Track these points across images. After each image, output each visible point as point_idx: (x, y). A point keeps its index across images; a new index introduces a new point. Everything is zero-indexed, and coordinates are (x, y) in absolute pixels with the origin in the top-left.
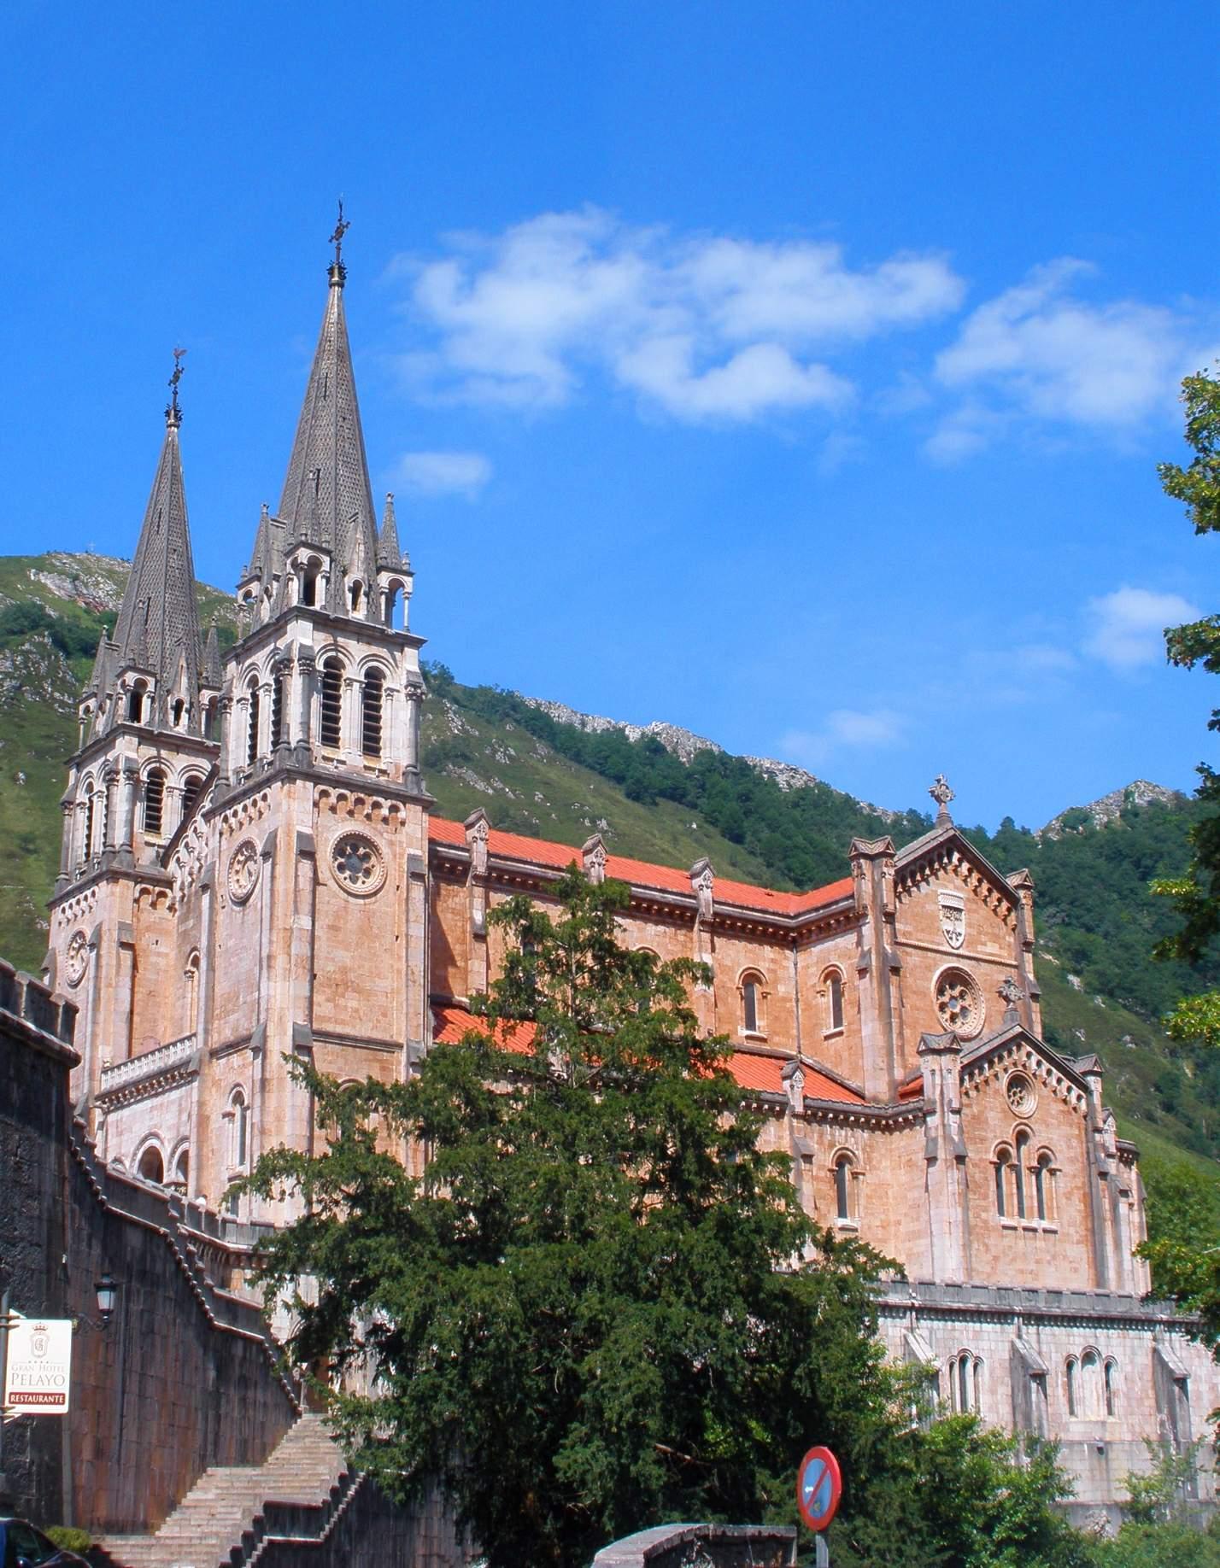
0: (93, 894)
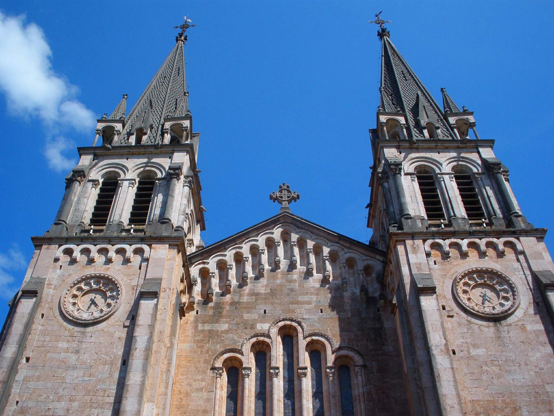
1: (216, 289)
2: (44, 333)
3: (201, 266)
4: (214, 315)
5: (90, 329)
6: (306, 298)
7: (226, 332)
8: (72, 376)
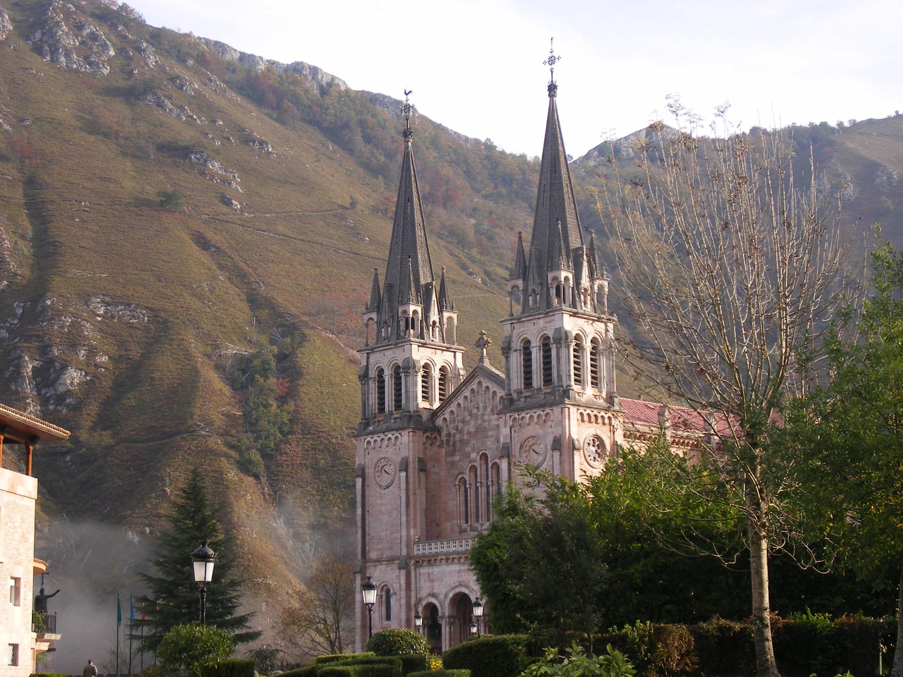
0: (397, 438)
5: (386, 491)
6: (490, 433)
7: (458, 461)
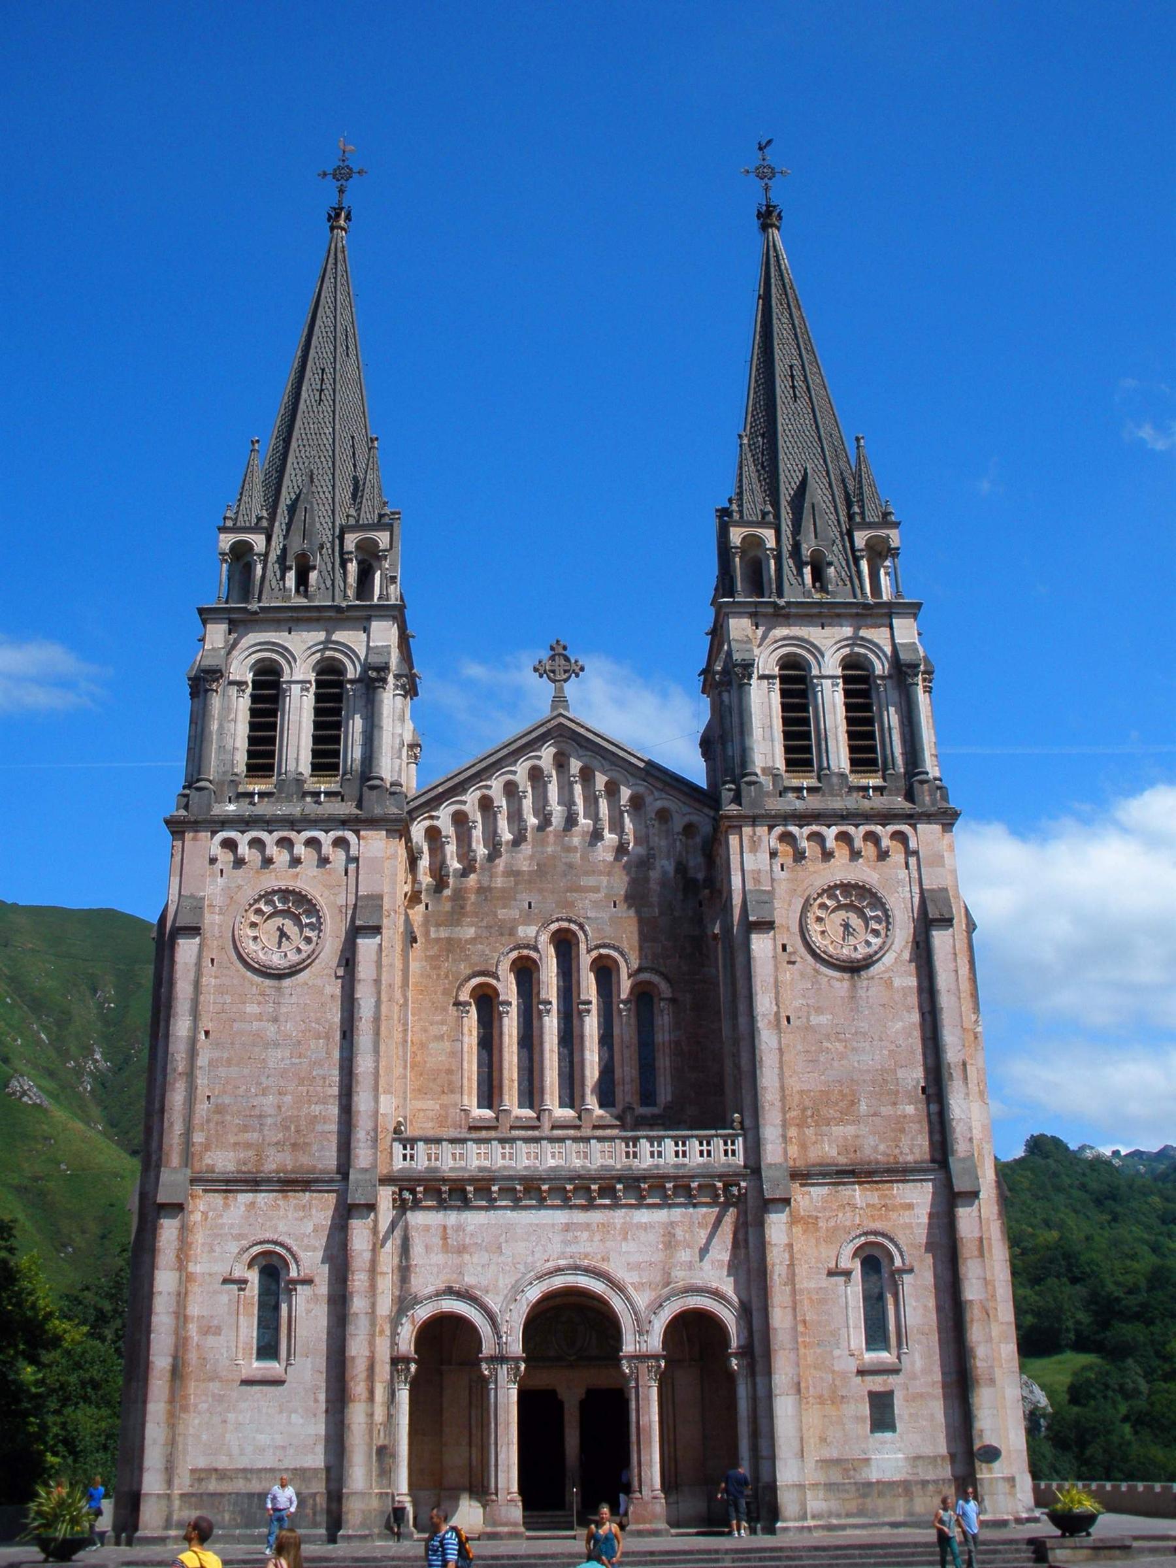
1: (454, 865)
2: (221, 990)
3: (427, 823)
4: (453, 912)
5: (287, 982)
7: (473, 940)
8: (277, 1058)
